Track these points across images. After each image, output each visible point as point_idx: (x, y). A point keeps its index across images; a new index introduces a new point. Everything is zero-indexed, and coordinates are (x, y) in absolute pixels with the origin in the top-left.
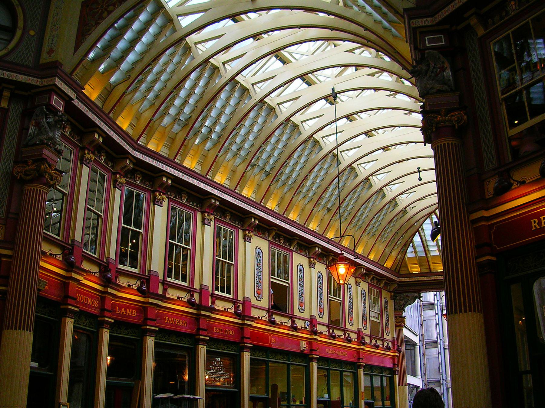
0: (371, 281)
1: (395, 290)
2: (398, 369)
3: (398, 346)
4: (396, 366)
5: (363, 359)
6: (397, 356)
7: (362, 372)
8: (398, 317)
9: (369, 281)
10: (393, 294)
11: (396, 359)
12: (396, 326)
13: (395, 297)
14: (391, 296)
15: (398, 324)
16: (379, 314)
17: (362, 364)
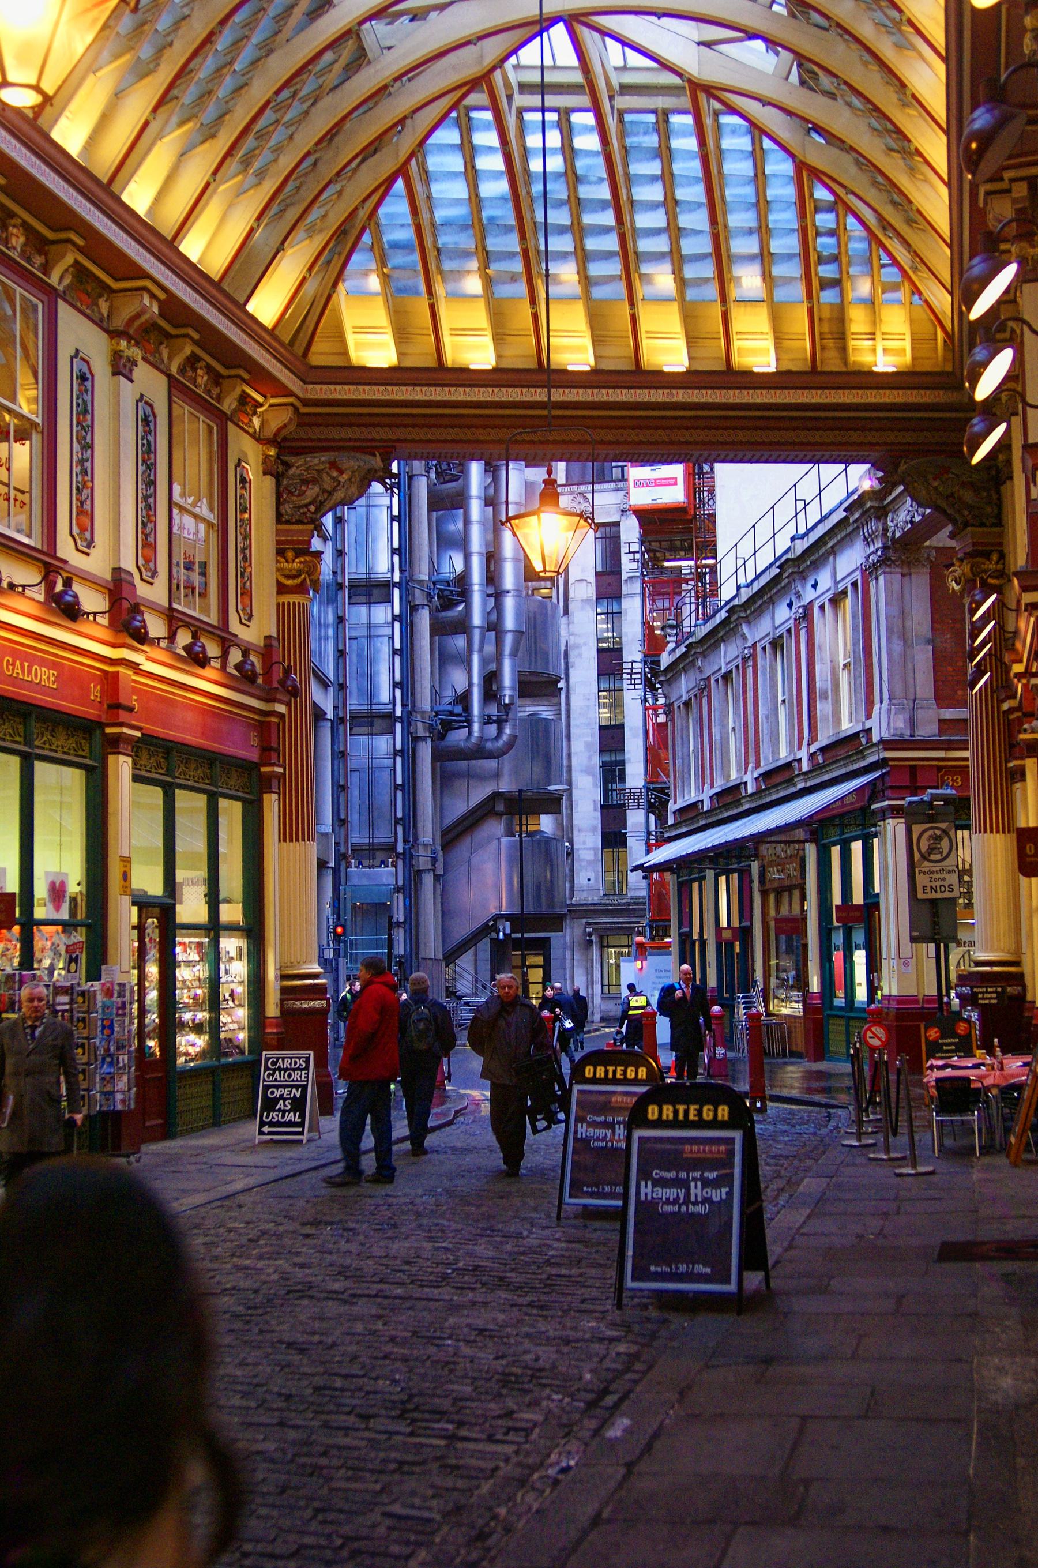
0: (182, 370)
1: (285, 439)
2: (281, 770)
3: (287, 671)
4: (274, 755)
5: (131, 710)
6: (281, 716)
7: (122, 767)
8: (290, 555)
9: (174, 370)
10: (272, 452)
11: (274, 730)
12: (281, 589)
13: (281, 469)
14: (266, 457)
15: (290, 582)
16: (209, 525)
17: (125, 730)
